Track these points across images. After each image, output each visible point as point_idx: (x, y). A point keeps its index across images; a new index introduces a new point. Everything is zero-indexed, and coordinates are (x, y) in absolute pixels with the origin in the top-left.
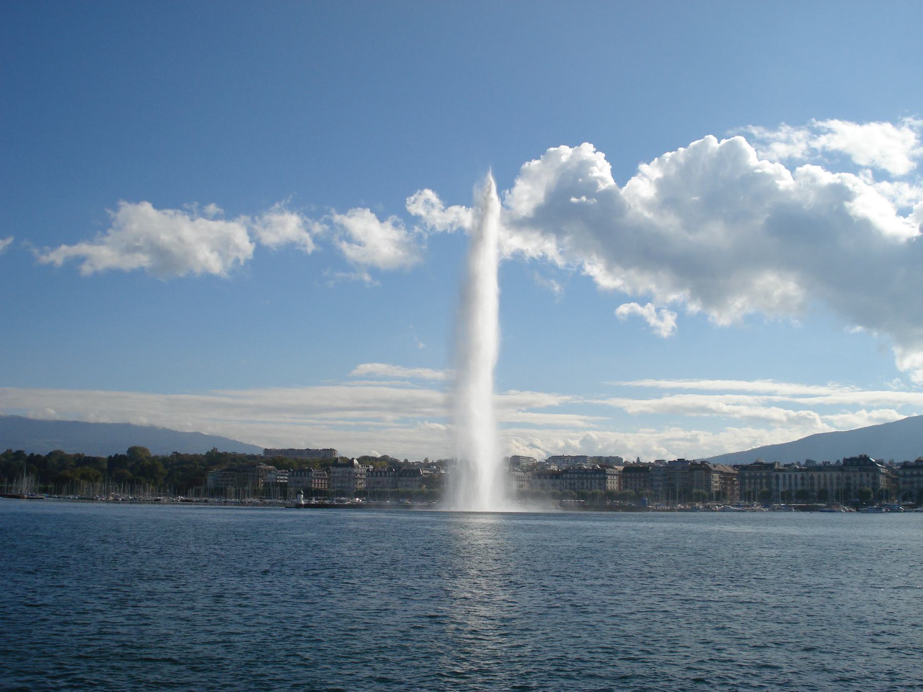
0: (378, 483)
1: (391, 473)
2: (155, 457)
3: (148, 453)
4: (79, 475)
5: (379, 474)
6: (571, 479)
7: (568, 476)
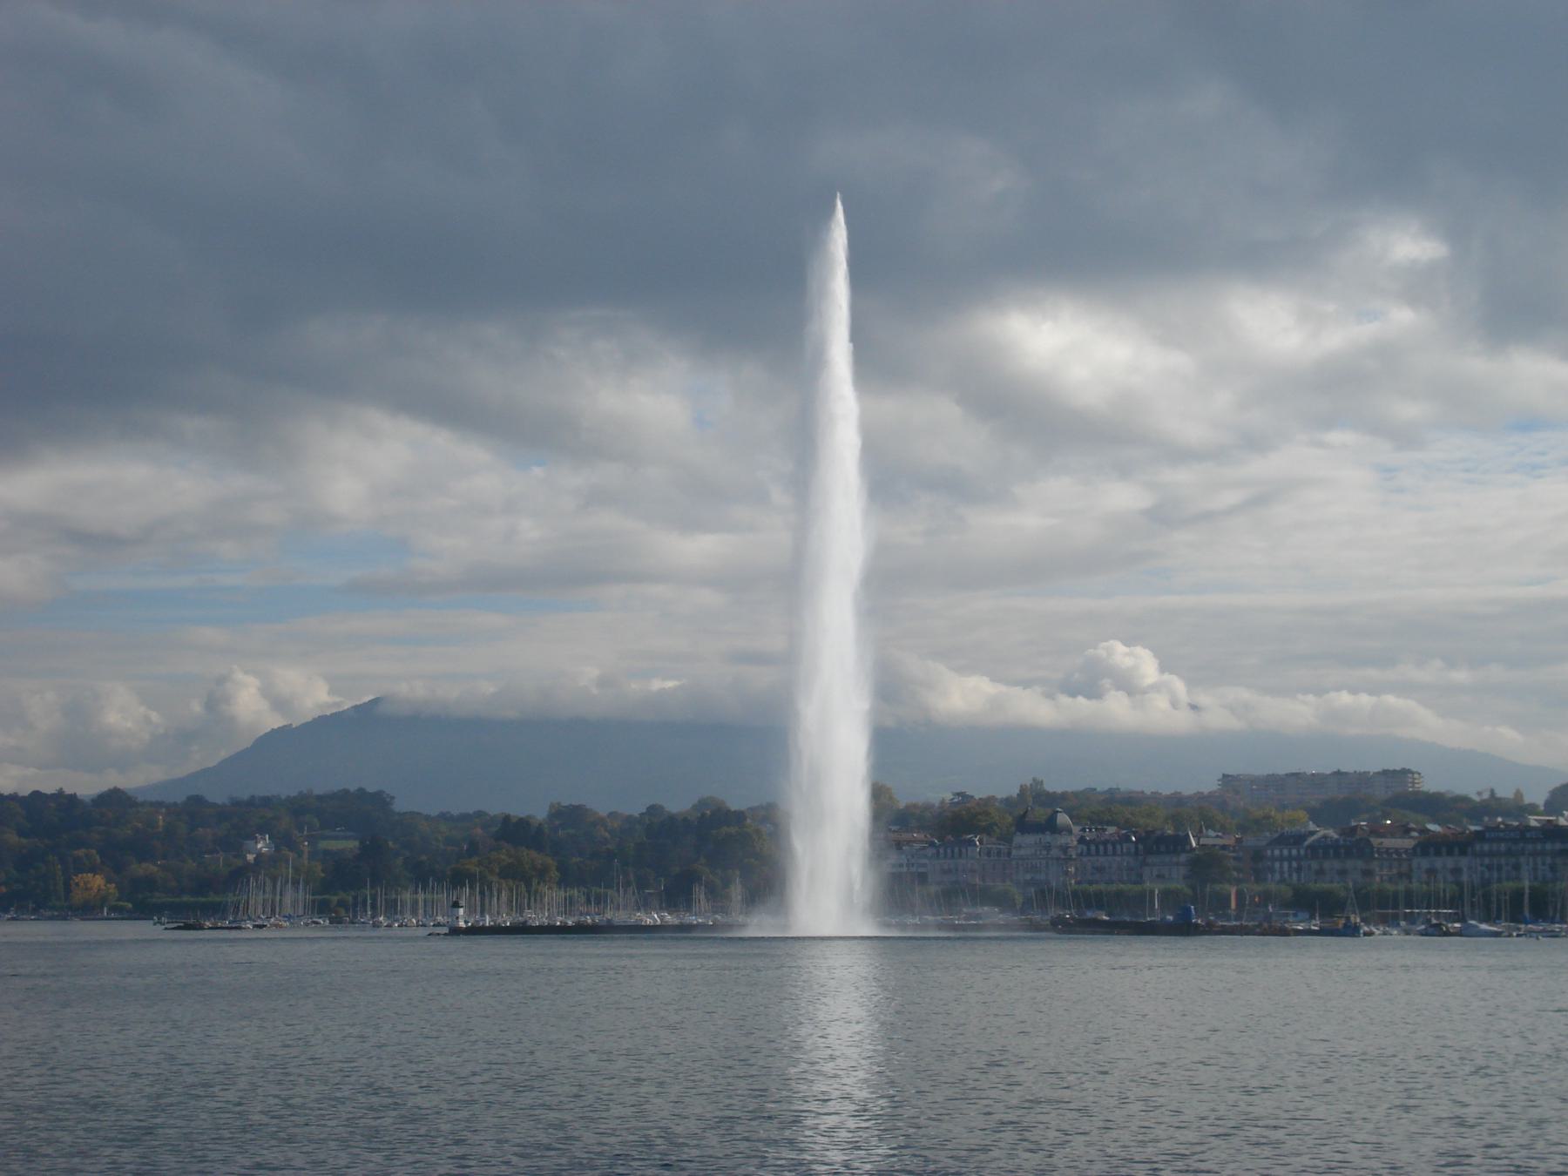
0: (1100, 870)
1: (1125, 846)
2: (907, 807)
3: (891, 798)
4: (497, 870)
5: (1101, 848)
6: (1491, 854)
7: (1486, 847)
